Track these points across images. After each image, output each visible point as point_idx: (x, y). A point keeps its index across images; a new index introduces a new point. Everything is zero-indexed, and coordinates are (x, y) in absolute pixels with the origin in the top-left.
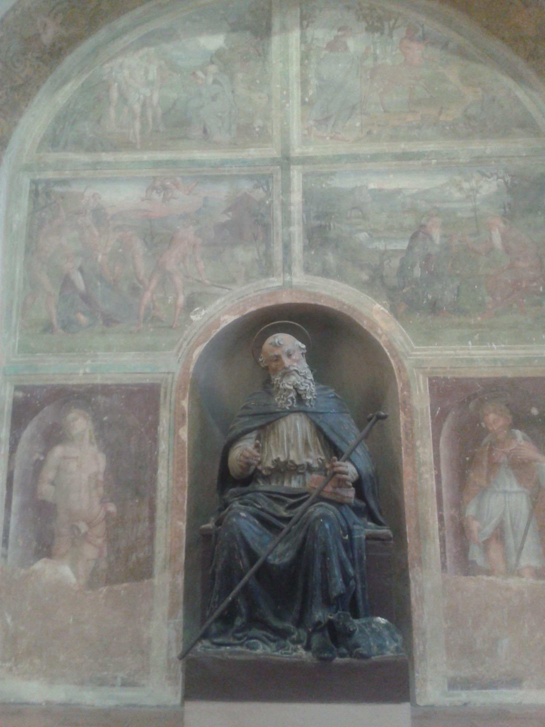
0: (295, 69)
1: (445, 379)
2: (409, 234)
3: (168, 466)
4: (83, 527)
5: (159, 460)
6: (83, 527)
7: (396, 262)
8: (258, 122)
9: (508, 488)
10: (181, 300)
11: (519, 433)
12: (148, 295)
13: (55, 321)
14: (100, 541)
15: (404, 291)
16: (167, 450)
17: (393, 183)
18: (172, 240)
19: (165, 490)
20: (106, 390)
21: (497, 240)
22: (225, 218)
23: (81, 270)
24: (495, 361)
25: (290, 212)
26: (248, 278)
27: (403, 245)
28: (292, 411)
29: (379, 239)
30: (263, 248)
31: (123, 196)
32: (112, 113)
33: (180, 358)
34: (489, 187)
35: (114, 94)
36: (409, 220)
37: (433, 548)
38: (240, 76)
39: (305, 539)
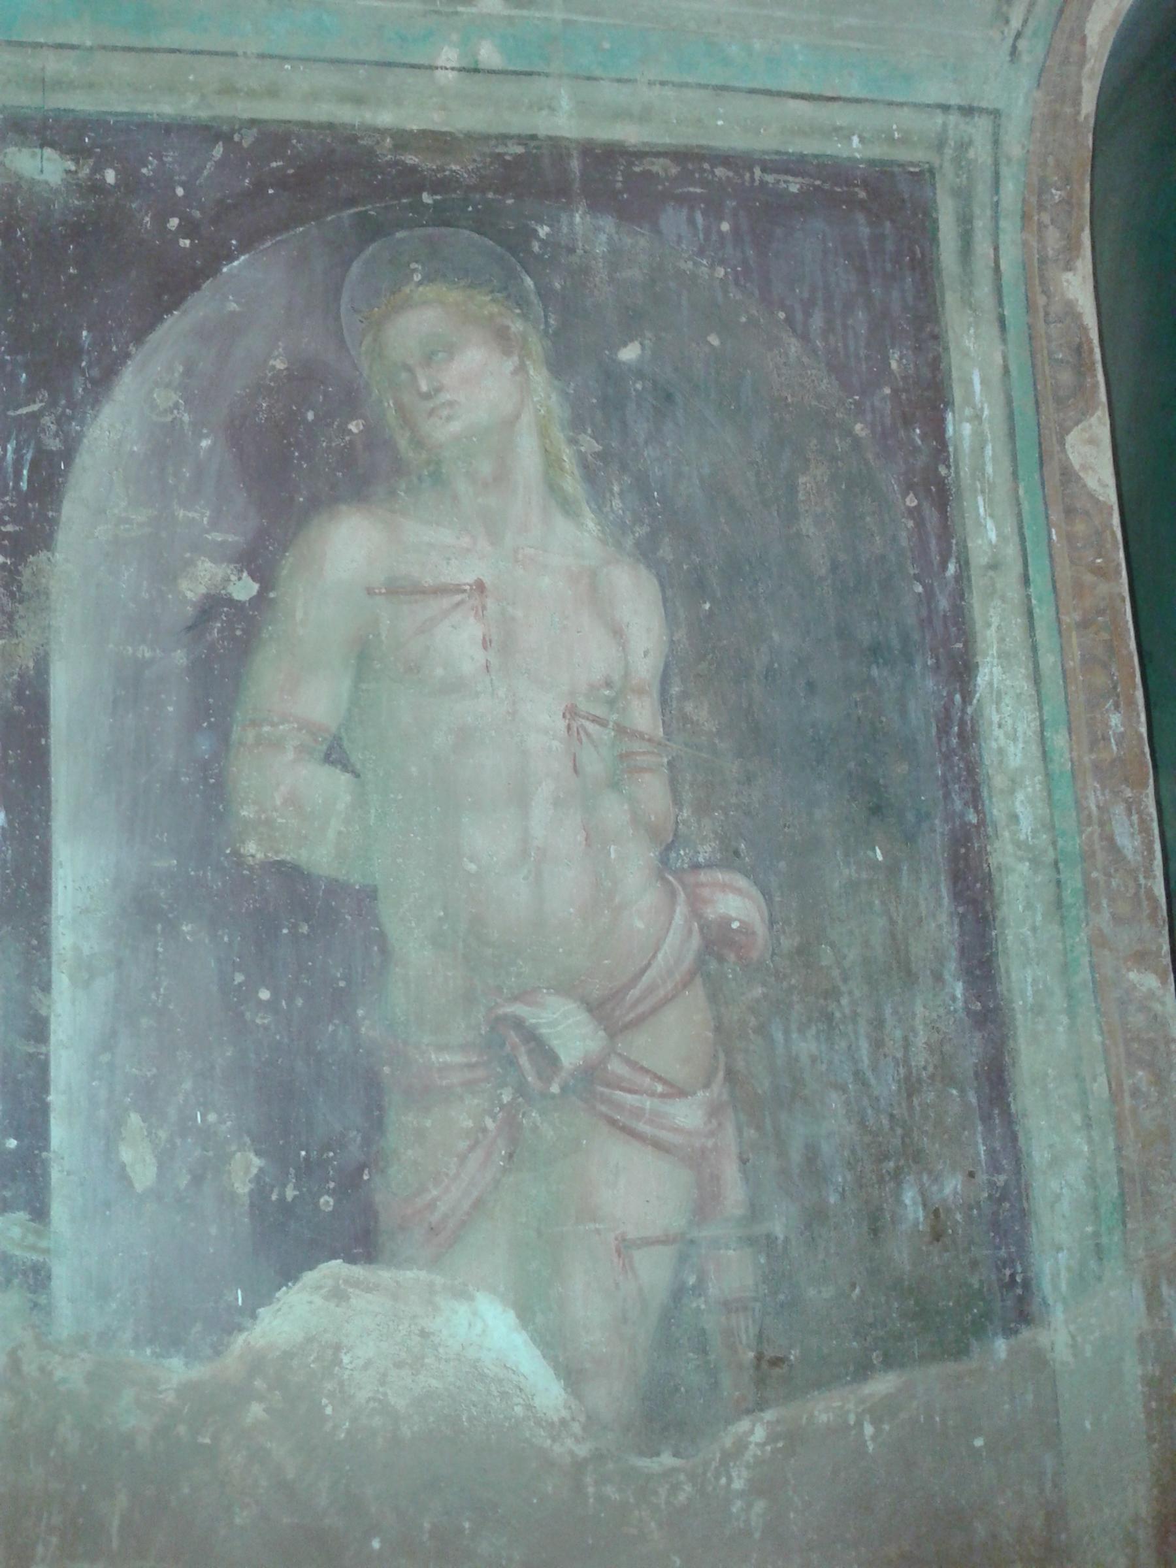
3: (1034, 648)
4: (572, 1035)
5: (976, 601)
6: (572, 1035)
14: (688, 1115)
16: (1011, 551)
19: (1032, 785)
20: (614, 178)
33: (1018, 35)
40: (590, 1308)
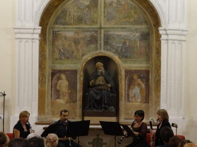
0: (103, 9)
1: (128, 70)
2: (123, 43)
4: (65, 94)
6: (65, 94)
7: (120, 48)
8: (95, 20)
9: (136, 88)
10: (81, 55)
11: (139, 79)
12: (75, 53)
13: (58, 58)
14: (67, 96)
15: (122, 54)
17: (120, 33)
18: (79, 43)
20: (68, 71)
21: (138, 45)
22: (89, 39)
23: (63, 48)
24: (136, 67)
25: (101, 38)
26: (93, 51)
27: (122, 45)
28: (101, 75)
29: (117, 44)
30: (96, 45)
31: (70, 34)
32: (68, 17)
34: (138, 35)
35: (68, 14)
36: (123, 41)
37: (123, 98)
38: (92, 11)
39: (102, 96)
40: (65, 101)
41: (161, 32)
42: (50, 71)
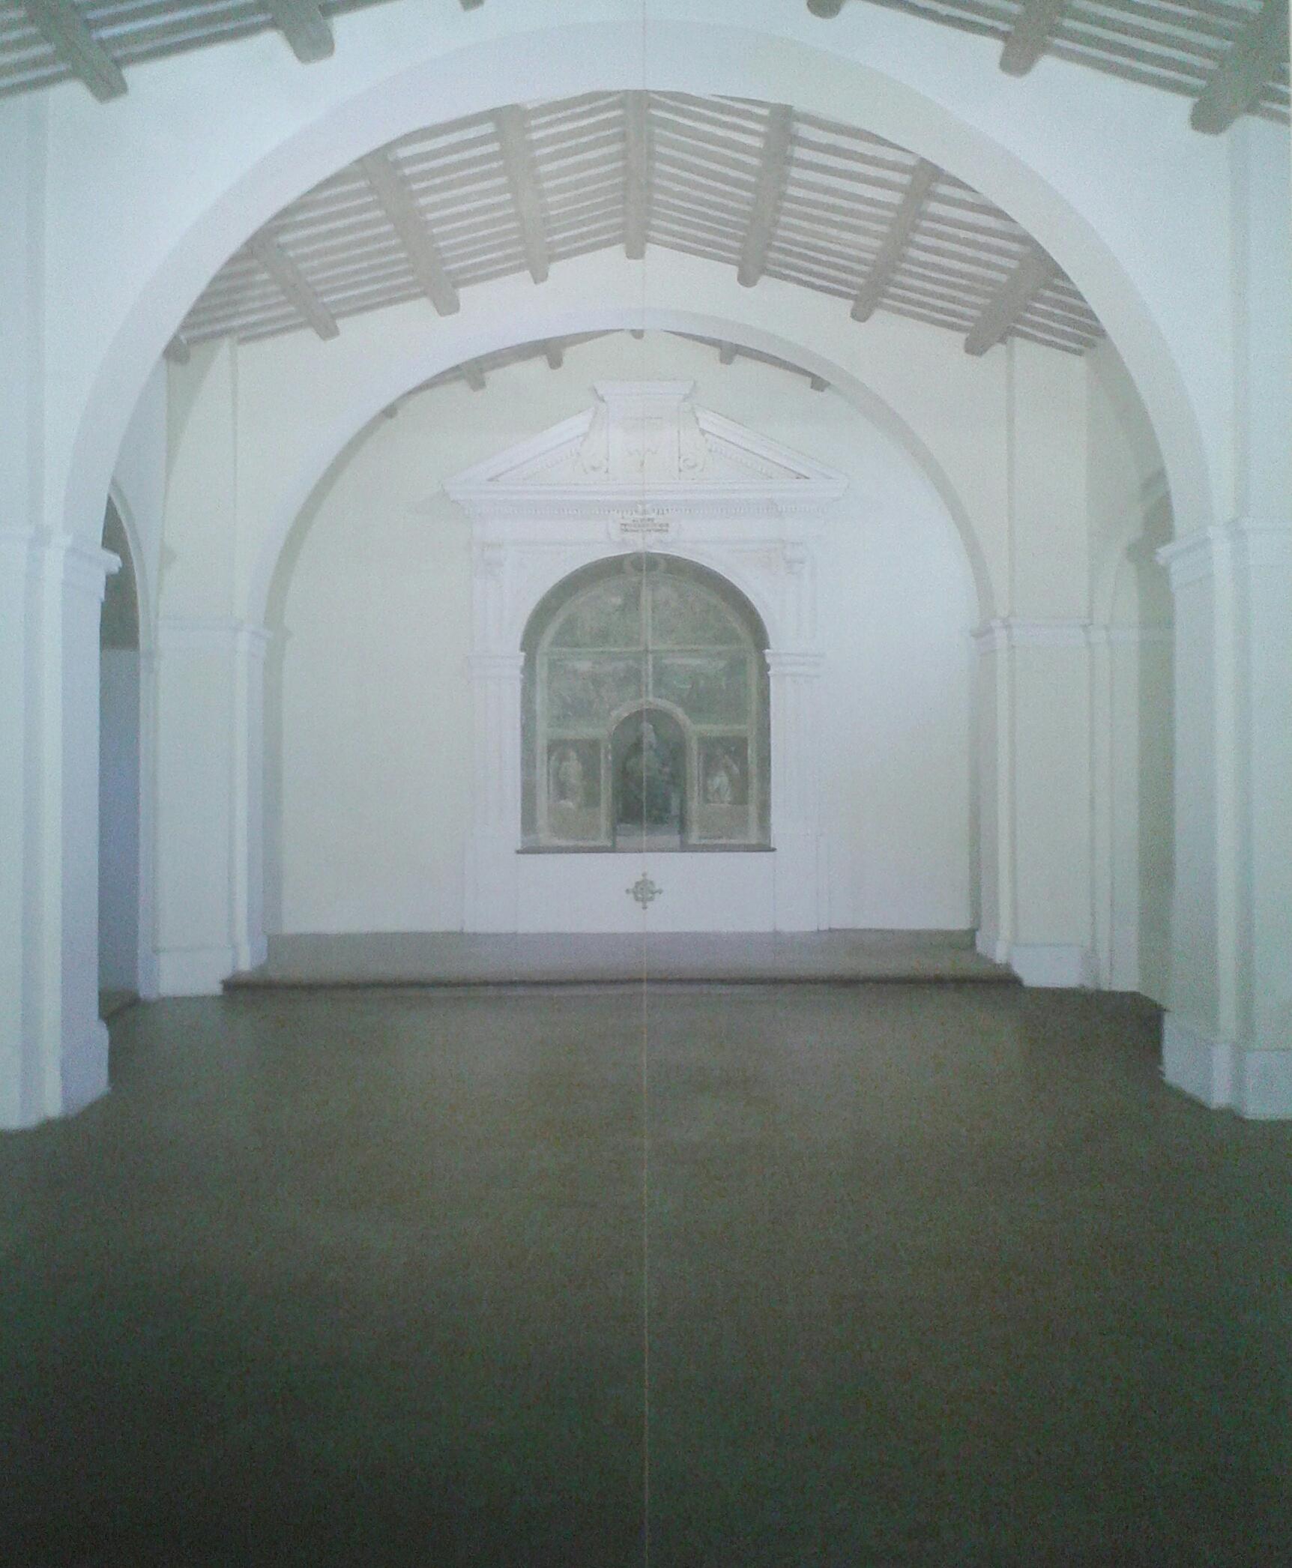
31: (584, 666)
34: (722, 664)
41: (768, 660)
42: (545, 742)
